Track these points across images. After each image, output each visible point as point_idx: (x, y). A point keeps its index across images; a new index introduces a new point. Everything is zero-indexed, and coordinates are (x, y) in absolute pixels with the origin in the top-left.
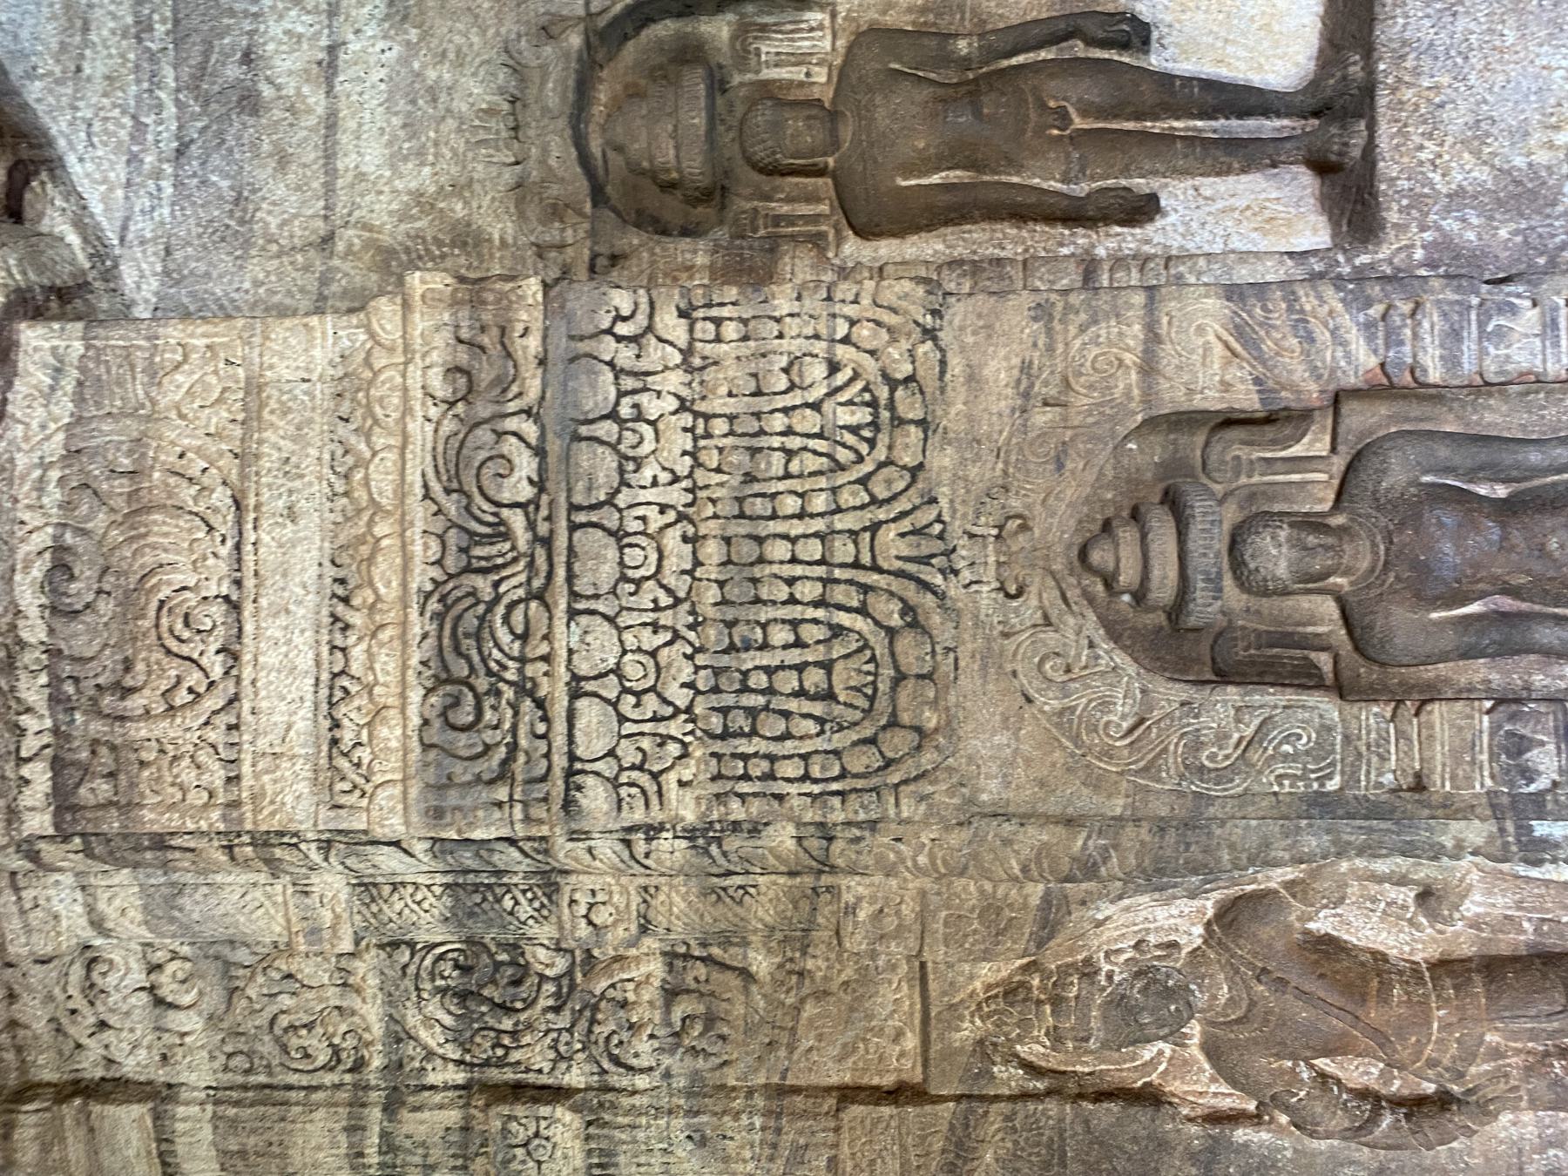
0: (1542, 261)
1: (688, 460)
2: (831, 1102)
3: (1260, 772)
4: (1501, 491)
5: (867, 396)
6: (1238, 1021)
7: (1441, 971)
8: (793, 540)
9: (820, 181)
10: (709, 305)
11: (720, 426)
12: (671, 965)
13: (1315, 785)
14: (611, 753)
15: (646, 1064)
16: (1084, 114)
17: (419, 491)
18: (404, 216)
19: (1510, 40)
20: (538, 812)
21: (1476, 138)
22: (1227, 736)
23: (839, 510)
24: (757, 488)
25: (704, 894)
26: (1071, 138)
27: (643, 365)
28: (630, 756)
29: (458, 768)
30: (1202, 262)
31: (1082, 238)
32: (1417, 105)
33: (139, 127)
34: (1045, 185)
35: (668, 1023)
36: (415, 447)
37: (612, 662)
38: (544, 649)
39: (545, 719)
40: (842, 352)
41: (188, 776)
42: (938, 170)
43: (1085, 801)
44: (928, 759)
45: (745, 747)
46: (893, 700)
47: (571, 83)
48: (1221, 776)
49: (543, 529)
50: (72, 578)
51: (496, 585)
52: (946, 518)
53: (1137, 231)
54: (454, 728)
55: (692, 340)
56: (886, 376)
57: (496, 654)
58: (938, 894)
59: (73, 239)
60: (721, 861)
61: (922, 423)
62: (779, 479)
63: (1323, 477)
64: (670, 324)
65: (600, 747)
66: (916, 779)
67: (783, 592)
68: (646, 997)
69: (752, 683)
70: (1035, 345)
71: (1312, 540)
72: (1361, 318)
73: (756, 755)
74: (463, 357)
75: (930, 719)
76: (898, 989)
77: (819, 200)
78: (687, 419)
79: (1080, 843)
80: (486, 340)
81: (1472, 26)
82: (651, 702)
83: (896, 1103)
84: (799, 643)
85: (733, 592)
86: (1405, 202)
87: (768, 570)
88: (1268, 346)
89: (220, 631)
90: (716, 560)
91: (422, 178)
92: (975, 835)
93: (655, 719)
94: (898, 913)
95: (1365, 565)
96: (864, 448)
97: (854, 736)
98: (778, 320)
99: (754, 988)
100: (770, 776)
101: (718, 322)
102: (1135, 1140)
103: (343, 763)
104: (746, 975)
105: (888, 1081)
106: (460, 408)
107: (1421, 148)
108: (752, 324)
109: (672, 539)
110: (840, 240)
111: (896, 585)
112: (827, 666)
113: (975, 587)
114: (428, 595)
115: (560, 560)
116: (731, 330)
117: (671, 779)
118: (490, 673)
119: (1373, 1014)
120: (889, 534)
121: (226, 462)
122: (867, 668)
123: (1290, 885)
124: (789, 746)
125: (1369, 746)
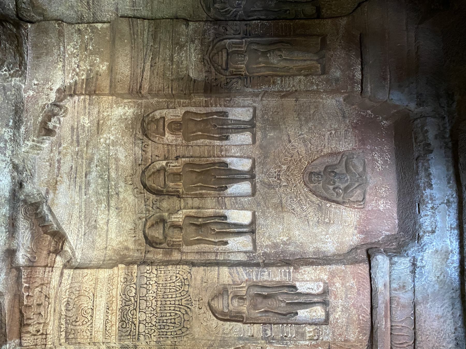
11: (161, 285)
14: (144, 331)
18: (117, 244)
19: (274, 223)
20: (134, 340)
27: (150, 277)
28: (147, 332)
29: (123, 333)
36: (119, 289)
40: (178, 275)
41: (85, 334)
43: (209, 338)
44: (188, 332)
48: (227, 334)
49: (136, 300)
50: (69, 305)
56: (183, 278)
59: (69, 251)
61: (188, 285)
65: (143, 331)
67: (169, 309)
71: (240, 301)
74: (126, 276)
75: (188, 326)
78: (156, 284)
82: (150, 324)
84: (171, 316)
85: (162, 309)
88: (234, 275)
89: (90, 313)
91: (121, 239)
93: (151, 326)
97: (178, 329)
101: (161, 271)
103: (107, 332)
106: (125, 283)
109: (154, 301)
111: (184, 307)
112: (175, 319)
115: (138, 304)
116: (163, 272)
120: (183, 300)
121: (92, 289)
124: (169, 330)
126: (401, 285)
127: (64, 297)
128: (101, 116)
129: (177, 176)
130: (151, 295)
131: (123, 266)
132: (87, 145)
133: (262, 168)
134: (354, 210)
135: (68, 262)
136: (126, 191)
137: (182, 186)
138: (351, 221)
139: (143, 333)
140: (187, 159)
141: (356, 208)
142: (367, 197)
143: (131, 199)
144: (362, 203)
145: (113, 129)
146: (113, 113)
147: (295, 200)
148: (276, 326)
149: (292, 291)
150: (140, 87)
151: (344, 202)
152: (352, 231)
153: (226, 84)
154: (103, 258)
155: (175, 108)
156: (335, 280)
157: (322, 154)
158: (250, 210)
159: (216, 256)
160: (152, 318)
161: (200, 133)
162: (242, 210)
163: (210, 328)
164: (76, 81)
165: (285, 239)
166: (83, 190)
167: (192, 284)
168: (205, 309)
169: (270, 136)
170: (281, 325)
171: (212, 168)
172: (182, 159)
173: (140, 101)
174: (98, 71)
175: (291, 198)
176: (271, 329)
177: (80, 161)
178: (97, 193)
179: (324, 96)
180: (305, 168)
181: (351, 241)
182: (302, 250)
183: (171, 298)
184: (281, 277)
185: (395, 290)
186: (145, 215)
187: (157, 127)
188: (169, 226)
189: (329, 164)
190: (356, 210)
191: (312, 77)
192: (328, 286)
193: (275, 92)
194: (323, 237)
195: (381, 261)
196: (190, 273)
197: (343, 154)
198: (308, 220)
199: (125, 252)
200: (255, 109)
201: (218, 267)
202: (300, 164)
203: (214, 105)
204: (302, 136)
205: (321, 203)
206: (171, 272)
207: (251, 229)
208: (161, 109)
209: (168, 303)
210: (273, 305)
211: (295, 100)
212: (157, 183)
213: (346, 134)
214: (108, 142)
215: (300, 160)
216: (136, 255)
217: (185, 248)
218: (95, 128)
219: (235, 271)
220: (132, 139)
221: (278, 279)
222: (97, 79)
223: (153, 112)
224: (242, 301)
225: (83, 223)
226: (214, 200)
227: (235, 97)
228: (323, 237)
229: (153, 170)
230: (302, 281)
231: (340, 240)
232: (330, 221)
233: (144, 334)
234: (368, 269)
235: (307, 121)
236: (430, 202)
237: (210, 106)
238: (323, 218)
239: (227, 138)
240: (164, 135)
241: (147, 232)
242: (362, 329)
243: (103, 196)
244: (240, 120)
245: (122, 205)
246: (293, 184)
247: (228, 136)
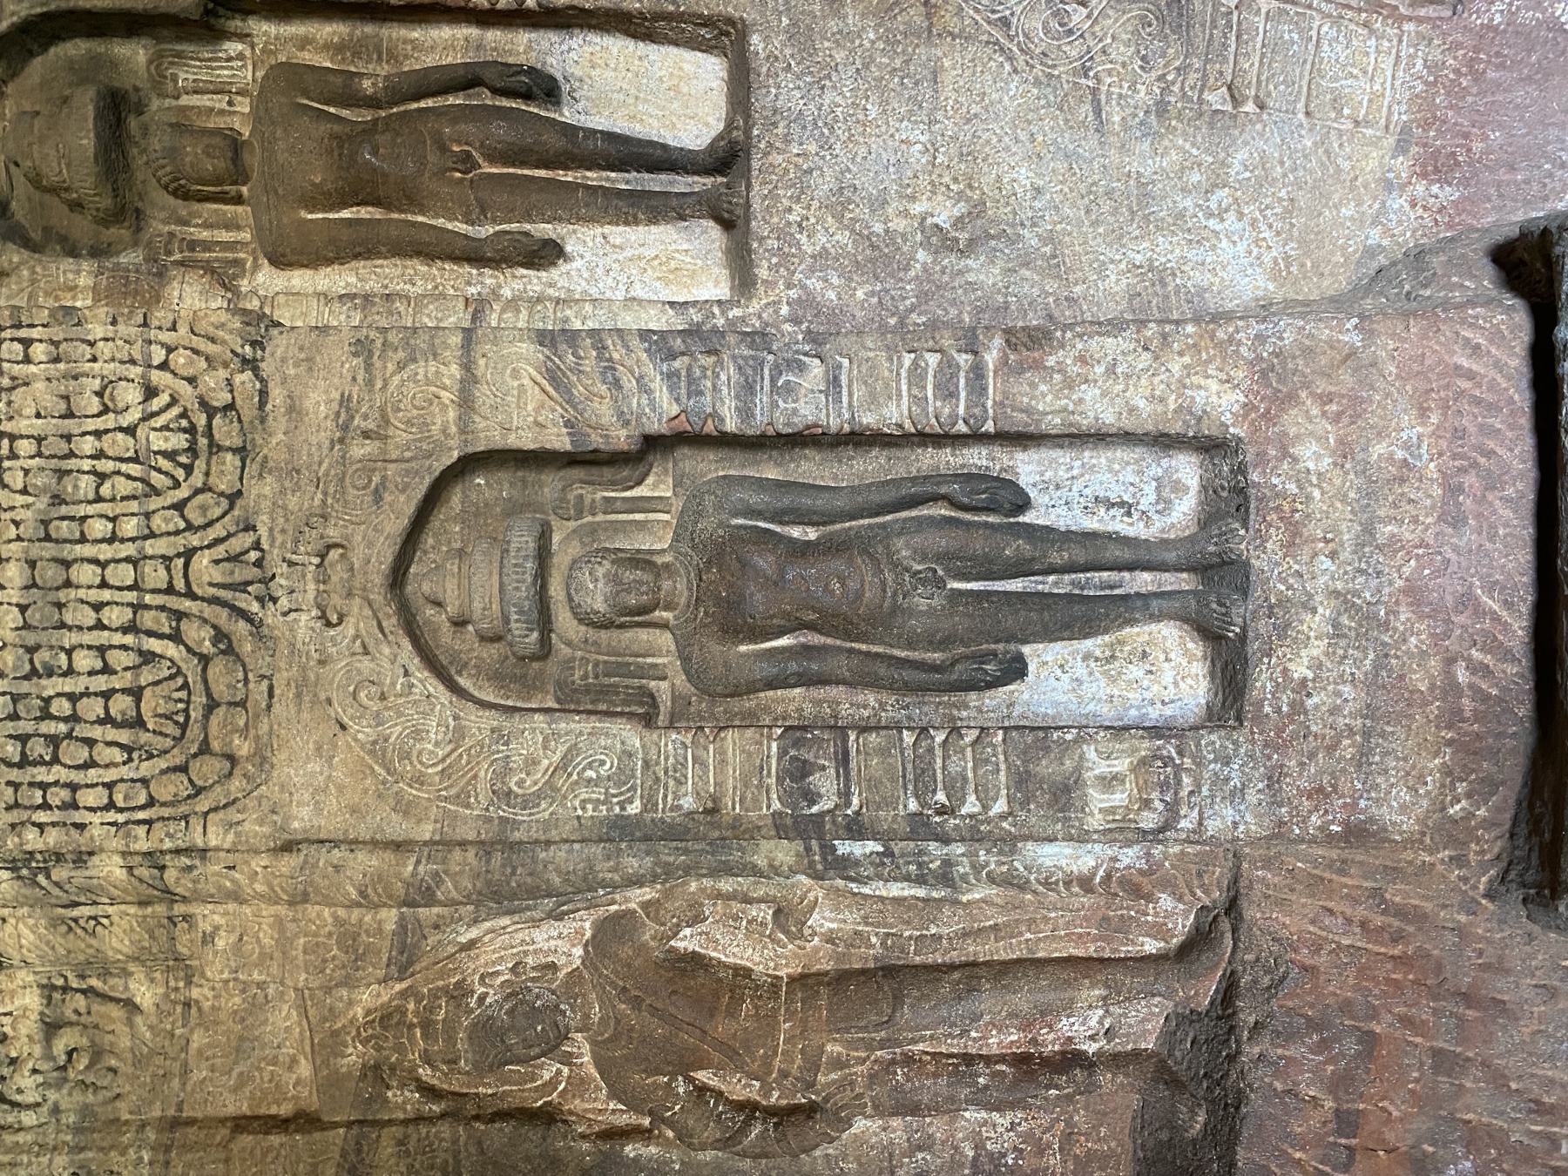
0: (892, 321)
2: (224, 1132)
3: (565, 797)
4: (812, 534)
5: (184, 423)
6: (610, 1040)
7: (797, 985)
8: (103, 565)
9: (240, 209)
10: (18, 326)
11: (25, 447)
12: (50, 998)
13: (617, 810)
15: (31, 1100)
16: (492, 159)
19: (873, 114)
21: (839, 203)
22: (535, 762)
23: (152, 535)
24: (64, 510)
25: (55, 923)
26: (472, 181)
30: (588, 307)
31: (490, 278)
32: (786, 171)
34: (449, 226)
35: (49, 1056)
40: (157, 377)
42: (345, 205)
43: (398, 827)
44: (236, 784)
45: (41, 774)
46: (205, 728)
48: (527, 802)
52: (265, 547)
53: (544, 274)
56: (203, 404)
58: (294, 920)
60: (56, 891)
62: (90, 502)
63: (666, 517)
66: (225, 806)
67: (89, 617)
68: (24, 1031)
69: (53, 710)
70: (354, 379)
71: (629, 576)
72: (665, 368)
73: (56, 783)
75: (243, 748)
76: (287, 1017)
77: (239, 228)
79: (411, 868)
81: (839, 99)
83: (286, 1131)
84: (107, 670)
85: (34, 616)
86: (774, 260)
87: (72, 593)
88: (579, 391)
90: (19, 582)
92: (306, 862)
94: (258, 941)
95: (683, 600)
96: (180, 474)
97: (163, 764)
98: (92, 344)
99: (139, 1020)
101: (27, 343)
102: (528, 1159)
104: (131, 1006)
105: (285, 1110)
107: (790, 210)
108: (64, 346)
110: (256, 267)
111: (208, 611)
112: (136, 693)
113: (293, 615)
116: (38, 351)
119: (722, 1028)
120: (202, 561)
122: (177, 695)
123: (645, 905)
124: (93, 774)
125: (666, 773)
138: (1375, 98)
156: (1291, 421)
165: (944, 213)
168: (368, 627)
176: (843, 760)
190: (1409, 27)
192: (1241, 469)
194: (1188, 203)
198: (1095, 92)
206: (104, 349)
210: (859, 595)
219: (589, 364)
221: (894, 414)
228: (1188, 203)
232: (1236, 101)
238: (1193, 77)
242: (1467, 749)
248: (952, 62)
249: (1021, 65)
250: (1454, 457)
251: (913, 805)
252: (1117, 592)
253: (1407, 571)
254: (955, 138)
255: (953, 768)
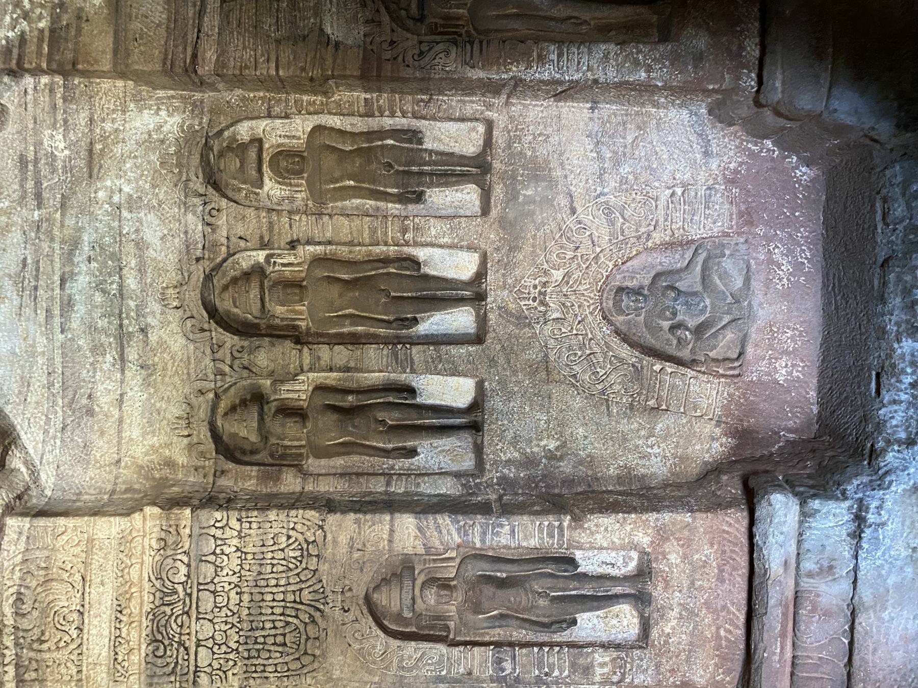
1: (239, 567)
8: (274, 594)
10: (248, 517)
11: (250, 557)
14: (210, 665)
17: (147, 579)
23: (289, 584)
24: (262, 577)
27: (224, 536)
28: (216, 665)
29: (158, 670)
33: (48, 419)
36: (146, 565)
37: (211, 635)
38: (188, 631)
39: (188, 654)
40: (291, 533)
44: (316, 665)
46: (306, 646)
47: (209, 410)
50: (23, 603)
51: (172, 610)
54: (156, 656)
55: (241, 528)
56: (306, 540)
57: (172, 632)
59: (23, 469)
64: (234, 523)
65: (206, 663)
67: (270, 611)
74: (163, 535)
75: (317, 652)
78: (239, 554)
80: (171, 530)
82: (224, 648)
84: (275, 628)
89: (76, 622)
93: (225, 653)
96: (298, 564)
100: (264, 671)
101: (250, 523)
103: (119, 667)
106: (162, 552)
109: (233, 594)
110: (308, 458)
112: (284, 635)
114: (149, 613)
115: (194, 602)
116: (254, 526)
117: (230, 673)
118: (169, 638)
120: (305, 592)
121: (80, 566)
124: (270, 661)
126: (826, 564)
127: (9, 583)
128: (98, 131)
129: (293, 287)
130: (225, 580)
131: (156, 510)
132: (63, 205)
133: (504, 275)
134: (716, 381)
135: (19, 497)
136: (164, 324)
137: (306, 313)
138: (709, 405)
139: (205, 669)
140: (319, 249)
141: (723, 376)
142: (750, 350)
143: (177, 343)
144: (736, 364)
145: (128, 165)
146: (127, 125)
147: (579, 353)
148: (524, 651)
149: (565, 571)
150: (194, 56)
151: (694, 360)
152: (709, 428)
153: (419, 56)
154: (109, 487)
155: (287, 117)
156: (667, 547)
157: (650, 244)
158: (472, 376)
159: (388, 484)
160: (228, 632)
161: (352, 183)
162: (454, 375)
163: (370, 654)
164: (23, 33)
165: (552, 445)
166: (57, 320)
167: (328, 552)
168: (358, 613)
169: (525, 195)
170: (536, 649)
171: (381, 271)
172: (307, 248)
173: (198, 96)
174: (81, 9)
175: (570, 349)
177: (45, 246)
178: (92, 328)
179: (663, 100)
180: (607, 277)
181: (707, 453)
182: (590, 473)
183: (276, 586)
184: (542, 539)
185: (810, 575)
186: (212, 385)
187: (242, 163)
188: (273, 410)
189: (664, 269)
191: (637, 48)
192: (650, 561)
193: (542, 81)
194: (641, 442)
195: (781, 508)
196: (321, 527)
197: (698, 246)
198: (607, 400)
199: (166, 472)
200: (490, 125)
201: (392, 513)
202: (594, 267)
203: (387, 113)
204: (602, 199)
205: (641, 361)
206: (275, 524)
207: (471, 421)
208: (252, 119)
209: (269, 597)
210: (520, 602)
211: (591, 108)
212: (245, 305)
213: (710, 196)
214: (116, 199)
215: (596, 258)
216: (191, 479)
217: (313, 464)
218: (83, 164)
220: (178, 194)
221: (533, 542)
222: (79, 30)
223: (232, 125)
224: (446, 592)
225: (60, 402)
226: (385, 352)
227: (441, 93)
228: (641, 442)
229: (232, 273)
230: (592, 548)
231: (680, 451)
233: (208, 670)
234: (745, 523)
235: (617, 163)
236: (909, 370)
237: (377, 114)
238: (643, 397)
239: (419, 198)
240: (261, 186)
241: (219, 423)
243: (107, 336)
244: (452, 154)
245: (156, 359)
246: (576, 315)
247: (422, 193)
248: (555, 390)
249: (580, 391)
250: (722, 560)
251: (537, 672)
252: (609, 593)
253: (705, 597)
254: (556, 418)
255: (551, 661)
